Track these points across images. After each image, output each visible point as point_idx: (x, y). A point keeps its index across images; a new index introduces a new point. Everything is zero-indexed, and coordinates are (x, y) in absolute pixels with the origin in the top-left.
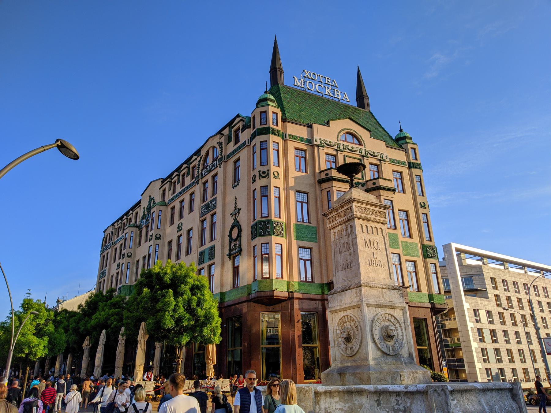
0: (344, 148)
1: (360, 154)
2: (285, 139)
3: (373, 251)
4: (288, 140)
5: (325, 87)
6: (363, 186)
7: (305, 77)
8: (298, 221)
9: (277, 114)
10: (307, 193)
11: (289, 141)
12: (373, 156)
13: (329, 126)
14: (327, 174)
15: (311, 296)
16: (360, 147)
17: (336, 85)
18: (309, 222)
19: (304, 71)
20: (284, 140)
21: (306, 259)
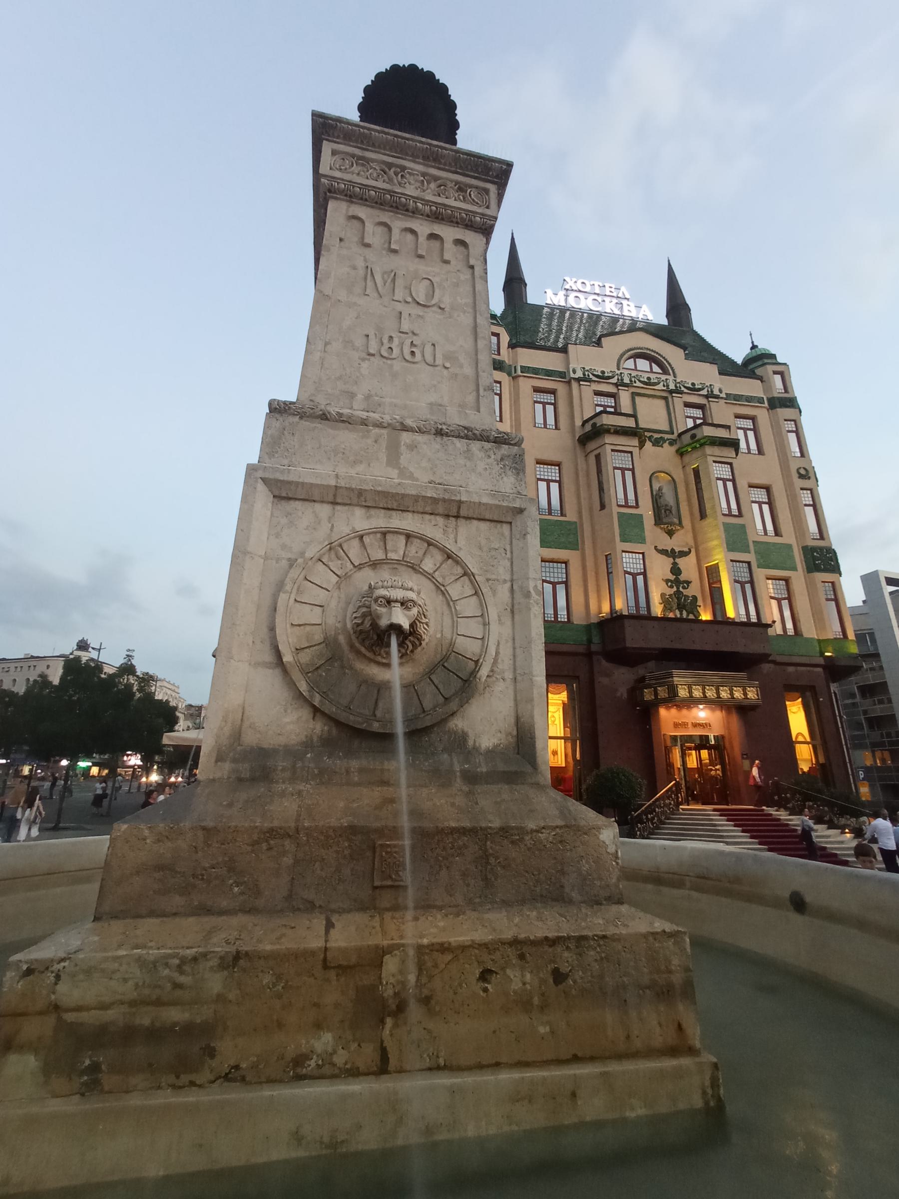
0: (631, 381)
1: (665, 388)
2: (514, 375)
3: (399, 307)
4: (520, 376)
5: (604, 301)
6: (671, 444)
7: (567, 290)
8: (540, 514)
9: (497, 335)
10: (558, 465)
11: (521, 378)
12: (693, 389)
13: (602, 347)
14: (594, 425)
15: (565, 648)
16: (664, 377)
17: (624, 295)
18: (562, 514)
19: (564, 280)
20: (513, 378)
21: (556, 580)
